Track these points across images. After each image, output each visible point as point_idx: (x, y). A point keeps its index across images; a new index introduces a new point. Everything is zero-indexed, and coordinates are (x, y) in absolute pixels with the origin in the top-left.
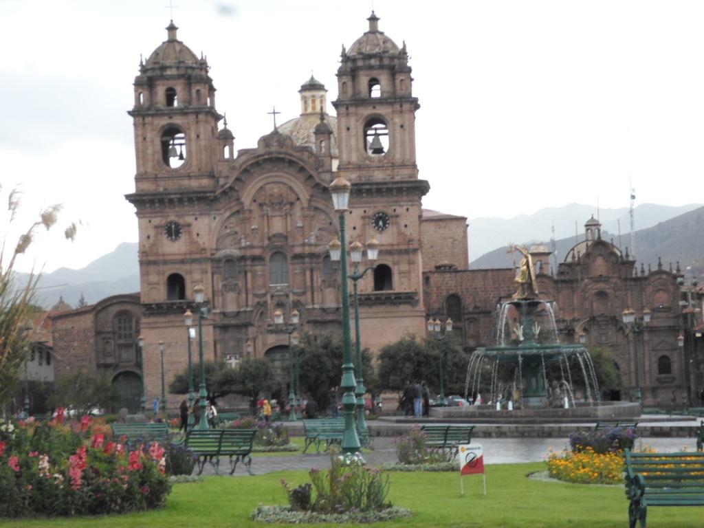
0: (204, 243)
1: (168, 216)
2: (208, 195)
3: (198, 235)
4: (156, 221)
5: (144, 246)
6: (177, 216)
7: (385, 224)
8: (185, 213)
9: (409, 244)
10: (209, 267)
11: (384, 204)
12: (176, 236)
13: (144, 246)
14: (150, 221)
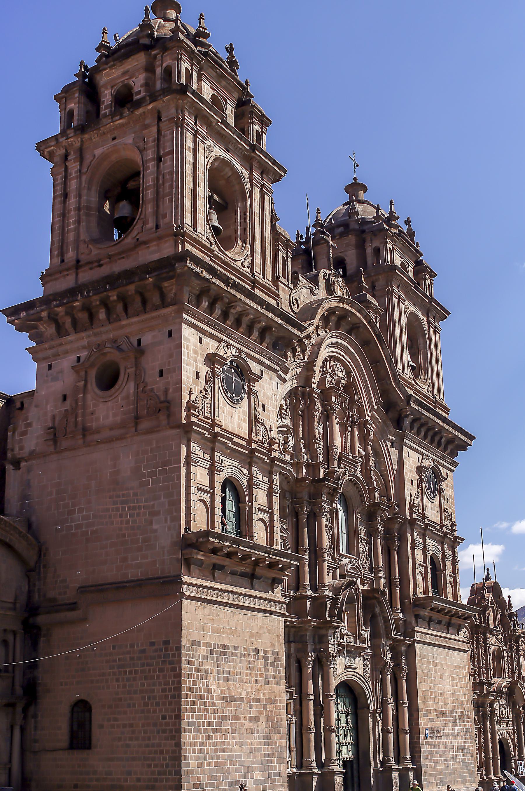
0: (270, 428)
1: (229, 345)
2: (296, 332)
3: (263, 406)
4: (211, 346)
5: (190, 394)
6: (239, 351)
7: (435, 489)
8: (252, 353)
9: (453, 531)
10: (276, 479)
11: (435, 458)
12: (238, 395)
13: (190, 394)
14: (200, 339)
